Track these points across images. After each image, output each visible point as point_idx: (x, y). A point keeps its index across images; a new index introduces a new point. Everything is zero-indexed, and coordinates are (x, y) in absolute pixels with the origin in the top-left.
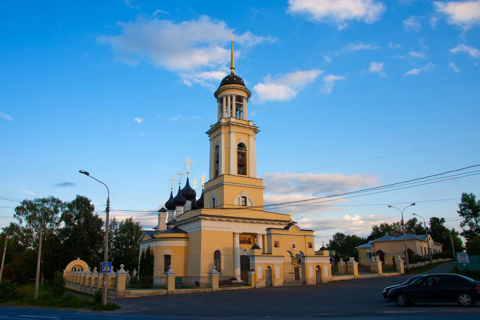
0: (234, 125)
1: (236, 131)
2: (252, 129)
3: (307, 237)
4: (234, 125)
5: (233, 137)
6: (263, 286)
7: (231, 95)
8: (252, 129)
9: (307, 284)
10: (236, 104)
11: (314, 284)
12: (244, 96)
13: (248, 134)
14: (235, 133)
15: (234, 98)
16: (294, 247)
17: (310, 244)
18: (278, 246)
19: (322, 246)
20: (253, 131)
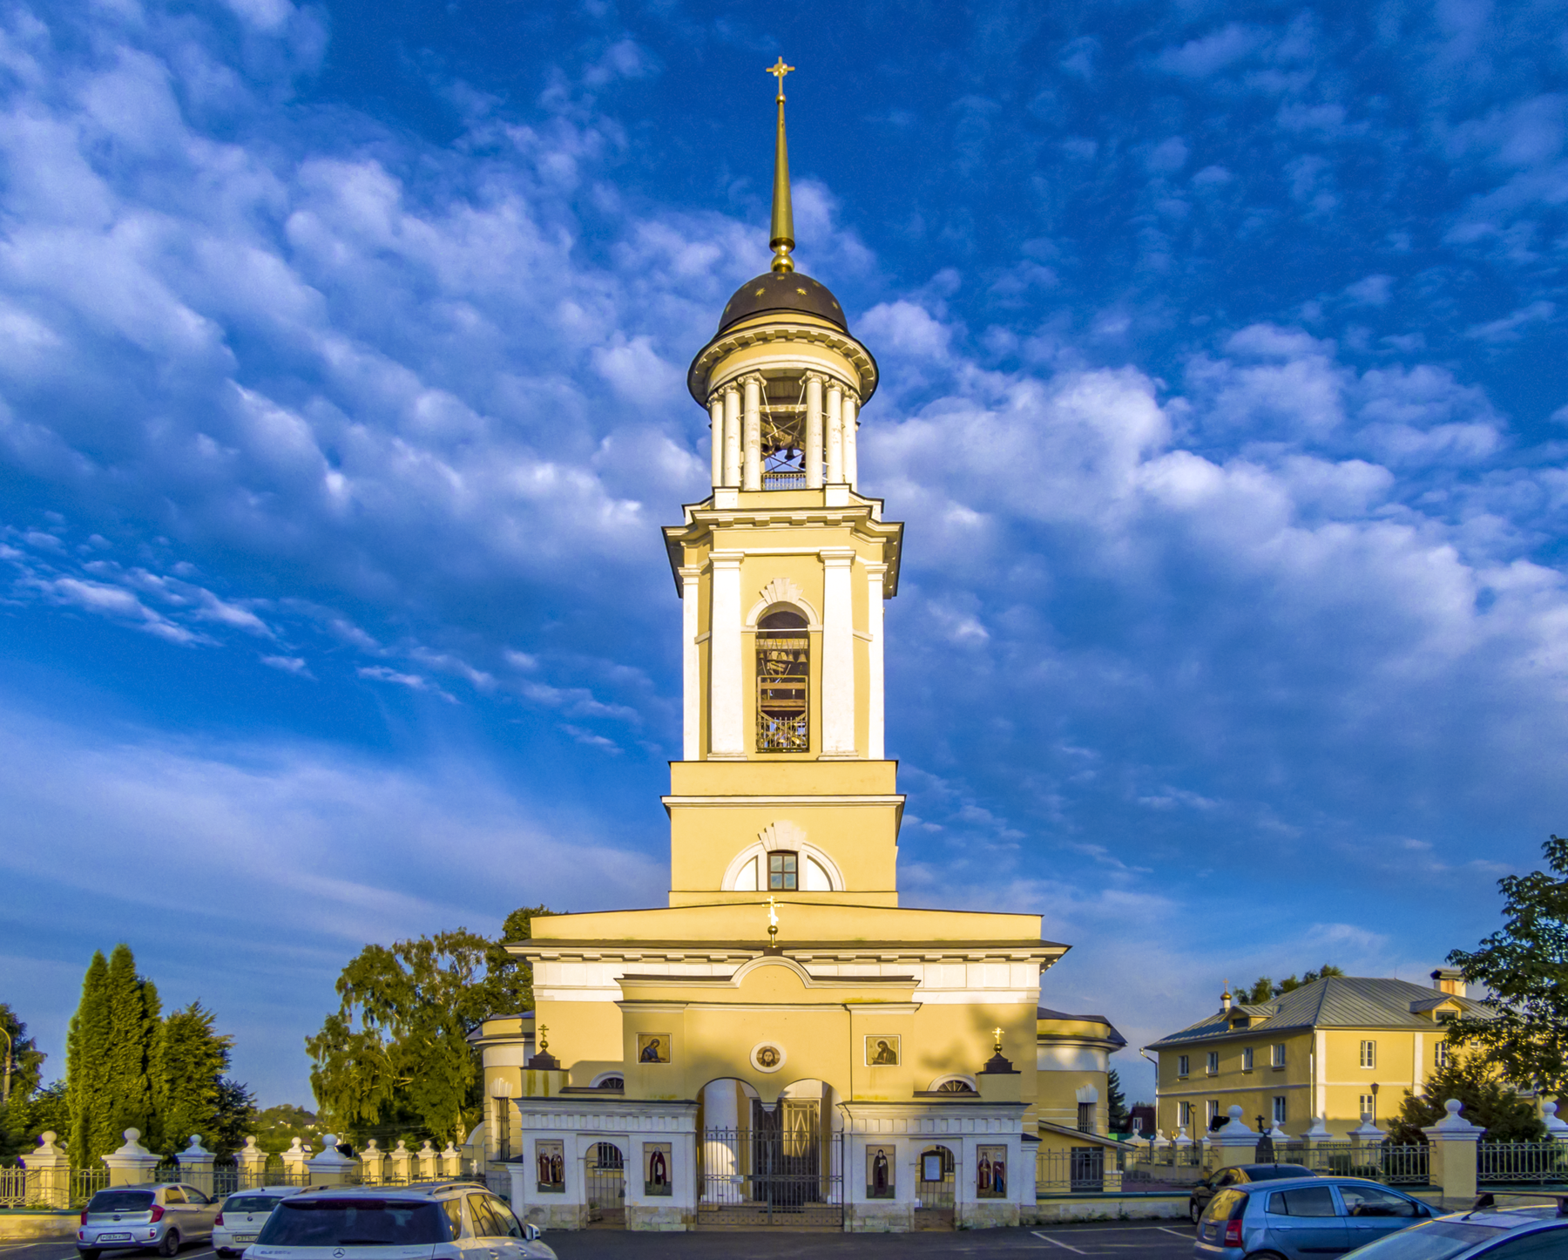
0: (728, 525)
1: (737, 551)
2: (836, 523)
3: (857, 1012)
4: (728, 525)
5: (728, 581)
6: (570, 1227)
7: (735, 379)
8: (836, 523)
9: (847, 1229)
10: (764, 417)
11: (896, 1229)
12: (802, 366)
13: (818, 555)
14: (736, 564)
15: (753, 391)
16: (768, 1057)
17: (882, 1043)
18: (660, 1055)
19: (995, 1053)
20: (845, 530)
